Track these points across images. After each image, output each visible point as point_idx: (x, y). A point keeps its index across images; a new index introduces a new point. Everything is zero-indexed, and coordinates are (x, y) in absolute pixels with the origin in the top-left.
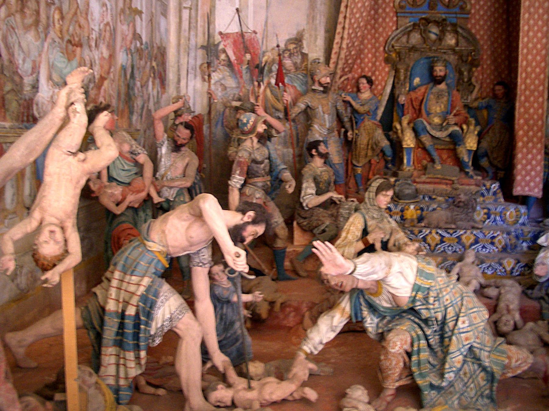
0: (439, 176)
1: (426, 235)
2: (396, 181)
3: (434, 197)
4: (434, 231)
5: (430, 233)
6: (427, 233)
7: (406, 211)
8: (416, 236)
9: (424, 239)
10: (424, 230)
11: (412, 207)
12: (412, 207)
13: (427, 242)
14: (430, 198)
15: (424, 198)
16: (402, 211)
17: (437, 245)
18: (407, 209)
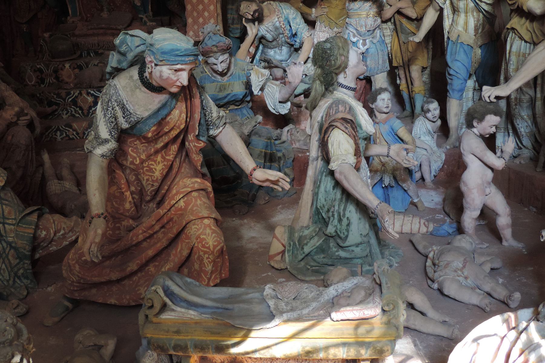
0: (103, 25)
1: (76, 97)
2: (51, 36)
3: (100, 51)
4: (84, 92)
5: (80, 94)
6: (76, 94)
7: (60, 71)
8: (64, 100)
9: (75, 102)
10: (72, 92)
11: (67, 66)
12: (67, 66)
13: (78, 105)
14: (96, 53)
15: (89, 54)
16: (56, 71)
17: (90, 108)
18: (62, 69)
